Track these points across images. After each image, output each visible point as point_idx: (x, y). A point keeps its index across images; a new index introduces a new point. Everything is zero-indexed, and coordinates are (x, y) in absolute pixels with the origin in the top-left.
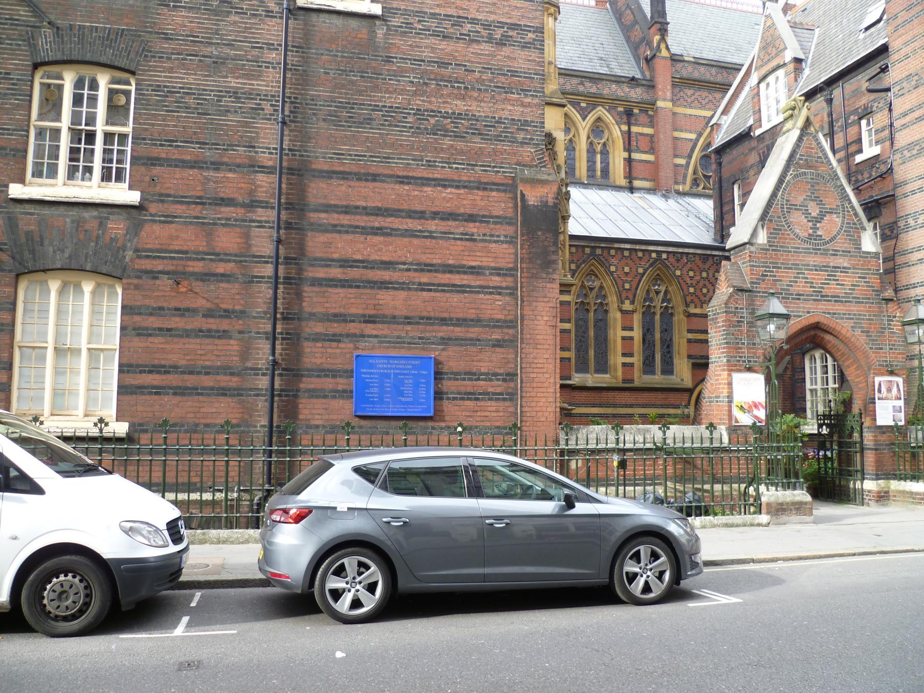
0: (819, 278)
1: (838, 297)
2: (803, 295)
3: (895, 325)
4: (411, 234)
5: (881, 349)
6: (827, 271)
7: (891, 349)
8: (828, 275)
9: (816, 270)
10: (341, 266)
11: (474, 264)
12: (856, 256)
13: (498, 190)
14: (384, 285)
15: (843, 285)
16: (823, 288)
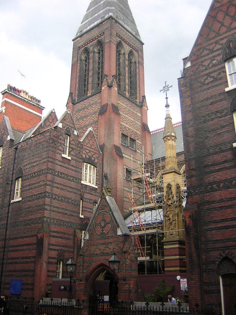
0: (102, 247)
1: (109, 253)
2: (98, 254)
3: (127, 262)
4: (21, 250)
5: (122, 271)
6: (105, 245)
7: (126, 271)
8: (106, 246)
9: (102, 245)
10: (12, 259)
11: (29, 256)
12: (115, 238)
13: (35, 236)
14: (16, 263)
15: (110, 249)
16: (104, 251)
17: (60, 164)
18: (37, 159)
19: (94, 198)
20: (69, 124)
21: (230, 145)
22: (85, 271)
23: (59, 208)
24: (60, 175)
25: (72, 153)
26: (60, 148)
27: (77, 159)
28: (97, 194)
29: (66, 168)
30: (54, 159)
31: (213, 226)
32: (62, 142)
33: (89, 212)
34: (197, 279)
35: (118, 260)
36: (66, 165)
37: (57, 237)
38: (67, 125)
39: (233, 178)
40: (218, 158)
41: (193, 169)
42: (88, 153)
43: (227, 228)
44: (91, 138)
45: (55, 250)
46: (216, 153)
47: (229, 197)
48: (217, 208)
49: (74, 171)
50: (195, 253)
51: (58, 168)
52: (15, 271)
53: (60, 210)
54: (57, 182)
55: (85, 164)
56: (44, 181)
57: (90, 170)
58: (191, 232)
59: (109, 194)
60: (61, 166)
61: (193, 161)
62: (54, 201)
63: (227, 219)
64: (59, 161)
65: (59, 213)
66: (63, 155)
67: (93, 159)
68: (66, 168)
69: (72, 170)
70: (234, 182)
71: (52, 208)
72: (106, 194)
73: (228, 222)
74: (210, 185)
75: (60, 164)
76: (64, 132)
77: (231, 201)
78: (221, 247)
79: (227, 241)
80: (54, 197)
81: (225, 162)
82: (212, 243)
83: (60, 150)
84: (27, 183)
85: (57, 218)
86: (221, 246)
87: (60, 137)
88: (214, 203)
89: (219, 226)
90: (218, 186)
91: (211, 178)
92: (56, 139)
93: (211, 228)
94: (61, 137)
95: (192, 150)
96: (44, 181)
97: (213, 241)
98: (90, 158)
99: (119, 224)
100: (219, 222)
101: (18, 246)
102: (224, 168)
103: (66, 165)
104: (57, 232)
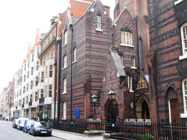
0: (111, 86)
4: (78, 92)
17: (95, 35)
18: (81, 35)
19: (131, 54)
20: (100, 8)
21: (173, 4)
22: (104, 101)
23: (96, 64)
24: (95, 43)
25: (104, 27)
26: (94, 25)
27: (108, 30)
28: (134, 51)
29: (100, 37)
30: (90, 33)
31: (163, 66)
32: (95, 21)
33: (128, 63)
34: (154, 103)
35: (114, 93)
36: (99, 36)
37: (97, 82)
38: (98, 9)
39: (175, 29)
40: (166, 16)
41: (153, 27)
42: (124, 24)
43: (170, 66)
44: (126, 13)
45: (95, 90)
46: (165, 12)
47: (172, 44)
48: (165, 52)
49: (106, 38)
50: (154, 86)
51: (94, 38)
52: (76, 104)
53: (97, 65)
54: (94, 47)
55: (123, 32)
56: (85, 48)
57: (127, 35)
58: (152, 71)
59: (114, 51)
60: (96, 36)
61: (153, 21)
62: (92, 60)
63: (171, 60)
64: (94, 34)
65: (97, 66)
66: (97, 30)
67: (129, 28)
68: (100, 37)
69: (104, 38)
70: (175, 32)
71: (91, 64)
72: (111, 51)
73: (171, 62)
74: (161, 36)
75: (95, 35)
76: (96, 14)
77: (173, 46)
78: (168, 80)
79: (171, 76)
80: (92, 57)
81: (170, 18)
82: (163, 78)
83: (94, 26)
84: (78, 50)
85: (95, 70)
86: (167, 79)
87: (93, 18)
88: (164, 49)
89: (166, 65)
90: (166, 36)
91: (162, 31)
92: (90, 20)
93: (162, 67)
94: (94, 18)
95: (152, 13)
96: (85, 48)
97: (163, 76)
98: (126, 28)
99: (118, 70)
100: (166, 63)
101: (77, 89)
102: (169, 23)
103: (99, 36)
104: (96, 79)
